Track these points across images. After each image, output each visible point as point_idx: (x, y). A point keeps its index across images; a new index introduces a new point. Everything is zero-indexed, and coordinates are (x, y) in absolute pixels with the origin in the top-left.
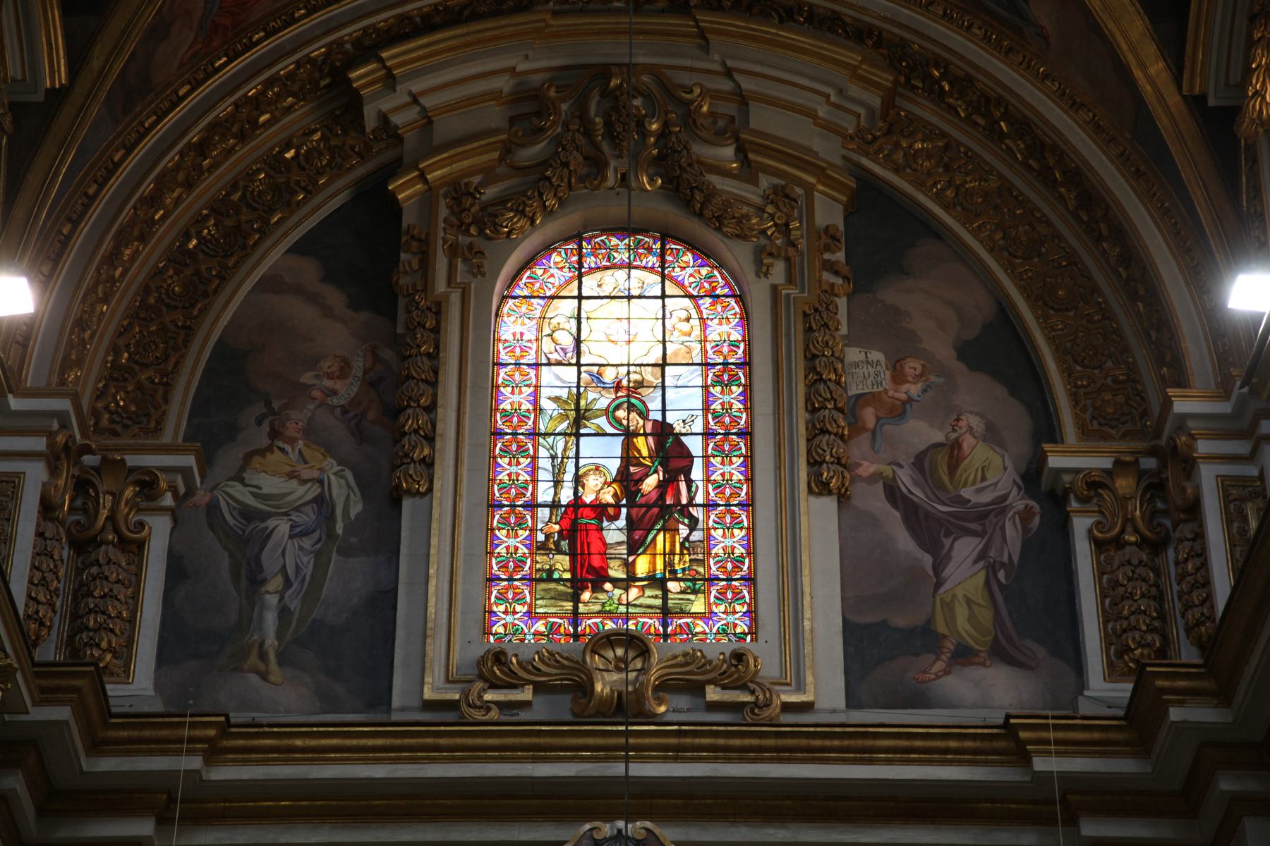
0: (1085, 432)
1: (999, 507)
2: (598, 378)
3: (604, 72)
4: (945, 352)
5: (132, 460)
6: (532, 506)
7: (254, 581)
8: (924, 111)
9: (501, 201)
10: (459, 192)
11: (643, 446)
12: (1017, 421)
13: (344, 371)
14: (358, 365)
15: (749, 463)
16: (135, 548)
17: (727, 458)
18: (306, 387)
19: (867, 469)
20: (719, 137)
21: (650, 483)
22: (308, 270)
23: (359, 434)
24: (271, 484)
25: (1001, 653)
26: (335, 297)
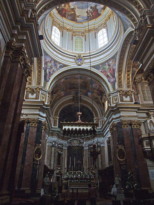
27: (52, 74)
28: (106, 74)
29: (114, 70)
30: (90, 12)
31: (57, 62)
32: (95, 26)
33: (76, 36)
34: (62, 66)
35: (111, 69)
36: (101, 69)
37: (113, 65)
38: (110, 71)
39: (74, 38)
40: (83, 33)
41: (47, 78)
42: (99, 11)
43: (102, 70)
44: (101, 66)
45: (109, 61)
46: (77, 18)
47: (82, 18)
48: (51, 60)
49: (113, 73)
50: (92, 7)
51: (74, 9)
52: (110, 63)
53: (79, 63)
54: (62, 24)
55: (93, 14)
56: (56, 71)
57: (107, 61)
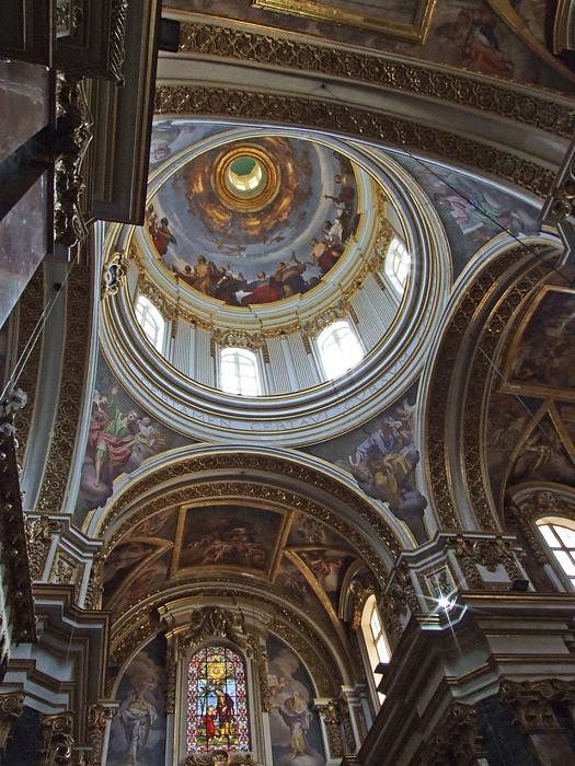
0: (321, 696)
1: (304, 713)
2: (211, 682)
3: (213, 609)
4: (288, 675)
5: (105, 705)
6: (197, 716)
7: (130, 737)
8: (282, 620)
9: (190, 639)
10: (180, 635)
11: (222, 700)
12: (305, 691)
13: (154, 679)
14: (157, 678)
15: (247, 704)
16: (103, 729)
17: (242, 703)
18: (143, 686)
19: (274, 705)
20: (239, 623)
21: (224, 709)
22: (145, 655)
23: (156, 697)
24: (135, 711)
25: (307, 753)
26: (151, 662)
29: (126, 464)
30: (153, 221)
35: (122, 444)
37: (141, 446)
38: (115, 446)
44: (114, 391)
49: (115, 467)
50: (167, 224)
52: (142, 428)
57: (144, 413)
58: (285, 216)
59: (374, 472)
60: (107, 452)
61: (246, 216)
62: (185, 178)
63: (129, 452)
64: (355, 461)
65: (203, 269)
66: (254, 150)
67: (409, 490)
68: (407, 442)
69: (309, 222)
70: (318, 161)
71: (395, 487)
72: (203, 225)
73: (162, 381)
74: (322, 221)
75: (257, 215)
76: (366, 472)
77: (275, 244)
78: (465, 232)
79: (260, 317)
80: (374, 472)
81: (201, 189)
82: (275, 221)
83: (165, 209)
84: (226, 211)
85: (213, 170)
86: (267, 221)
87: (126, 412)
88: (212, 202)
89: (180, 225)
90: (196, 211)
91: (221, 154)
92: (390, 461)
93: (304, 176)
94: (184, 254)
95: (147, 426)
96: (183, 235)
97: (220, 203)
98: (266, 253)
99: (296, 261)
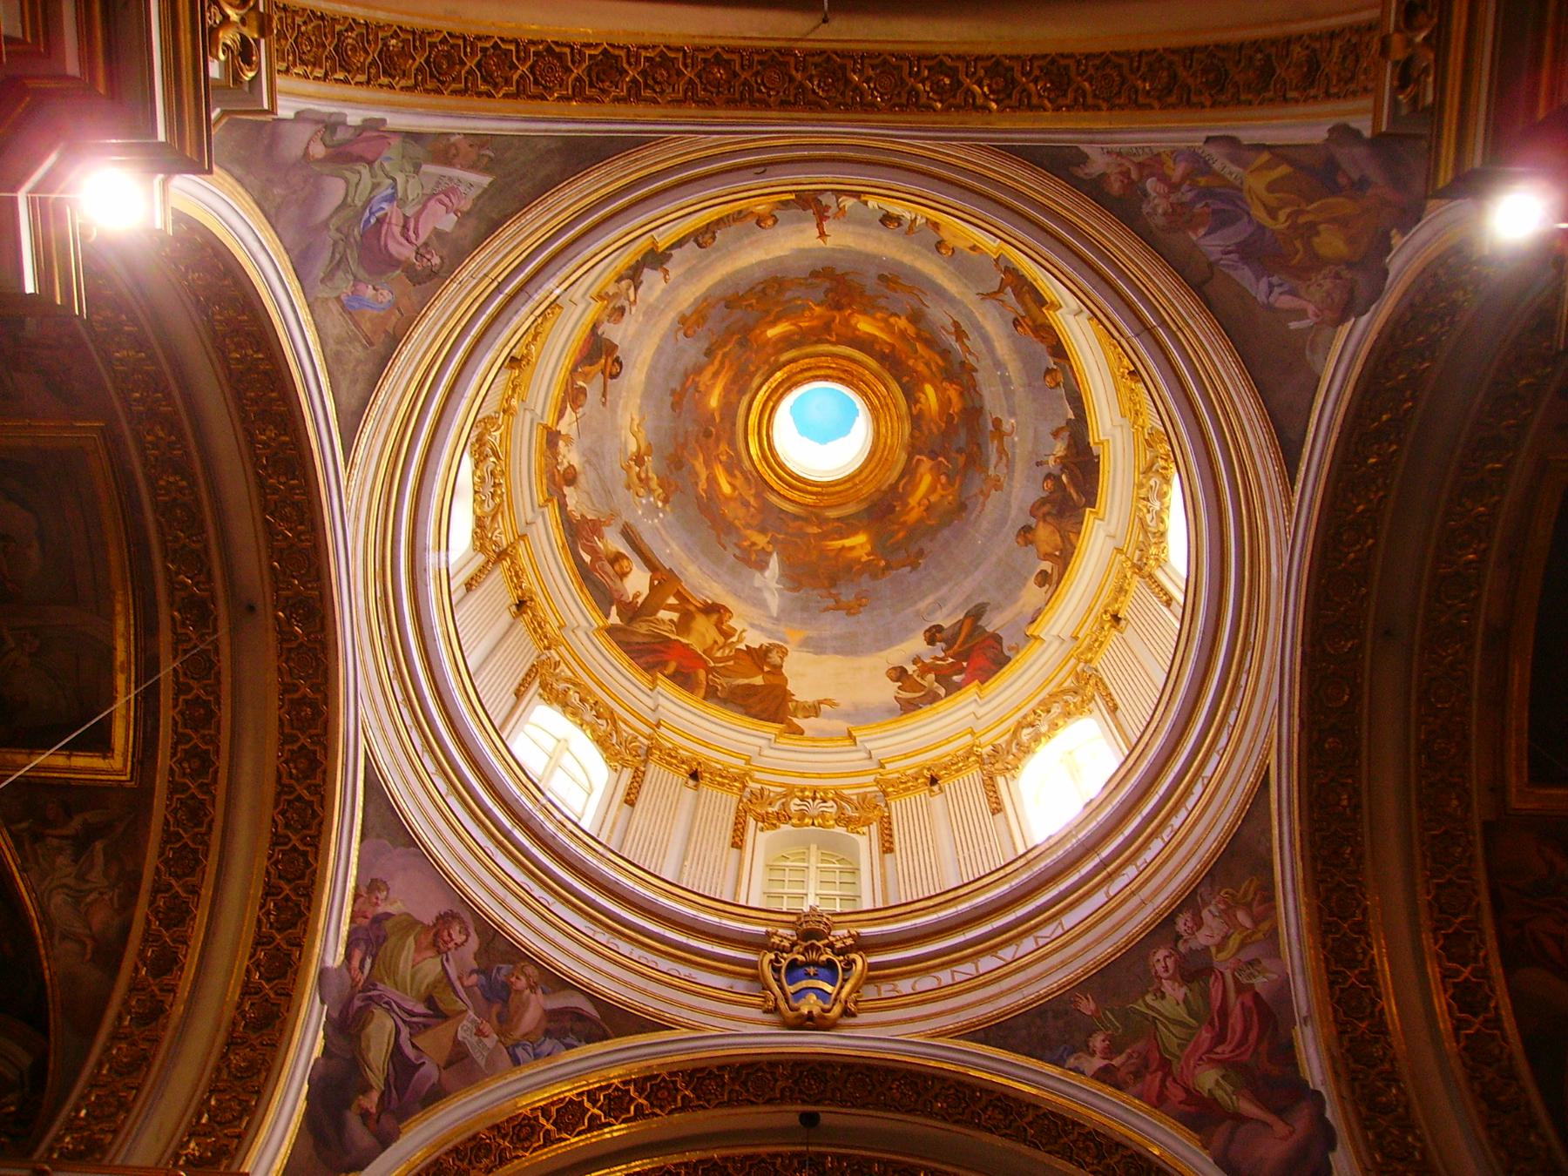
27: (436, 1096)
28: (1176, 1093)
30: (925, 669)
31: (516, 954)
32: (983, 740)
33: (785, 828)
34: (577, 1015)
35: (1224, 1012)
36: (1098, 1041)
37: (1245, 956)
39: (760, 841)
40: (864, 802)
41: (353, 1120)
42: (1005, 643)
43: (1111, 1050)
44: (1087, 1006)
45: (1182, 923)
46: (795, 720)
47: (846, 716)
48: (446, 919)
50: (939, 628)
51: (774, 657)
52: (1202, 938)
53: (810, 1005)
54: (647, 730)
55: (956, 678)
56: (491, 1062)
57: (1163, 929)
58: (902, 323)
59: (1316, 262)
60: (1228, 1065)
61: (916, 420)
62: (833, 581)
63: (1248, 999)
64: (1301, 314)
65: (1045, 534)
66: (753, 418)
67: (1332, 166)
68: (1199, 165)
69: (901, 264)
70: (737, 272)
71: (1343, 205)
72: (946, 533)
73: (1127, 832)
74: (885, 235)
75: (911, 395)
76: (1321, 288)
77: (973, 342)
78: (486, 180)
79: (1118, 419)
80: (1316, 262)
81: (860, 539)
82: (919, 346)
83: (905, 633)
84: (909, 472)
85: (813, 515)
86: (921, 367)
87: (1150, 982)
88: (891, 509)
89: (944, 590)
90: (914, 549)
91: (773, 499)
92: (1272, 214)
93: (788, 295)
94: (1009, 582)
95: (1199, 923)
96: (968, 585)
97: (893, 487)
98: (998, 365)
99: (1001, 290)
